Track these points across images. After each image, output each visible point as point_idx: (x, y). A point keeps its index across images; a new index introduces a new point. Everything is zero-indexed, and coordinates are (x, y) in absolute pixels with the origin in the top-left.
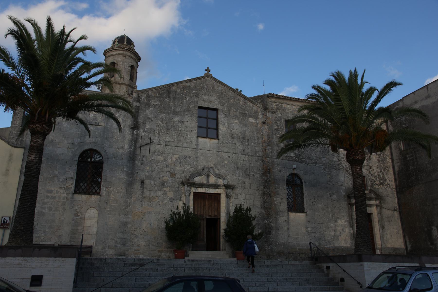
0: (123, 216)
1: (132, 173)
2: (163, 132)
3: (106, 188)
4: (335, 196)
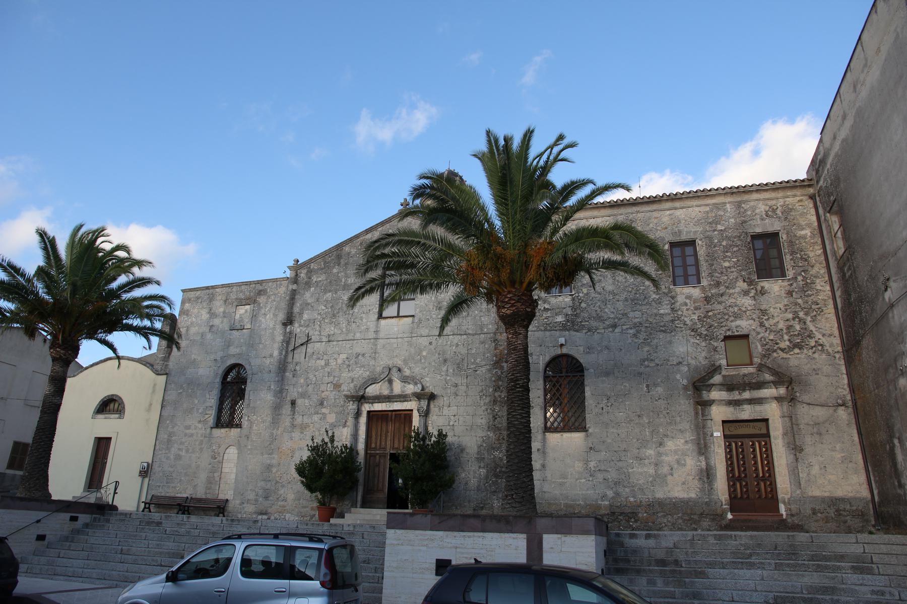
1: (281, 391)
4: (660, 390)
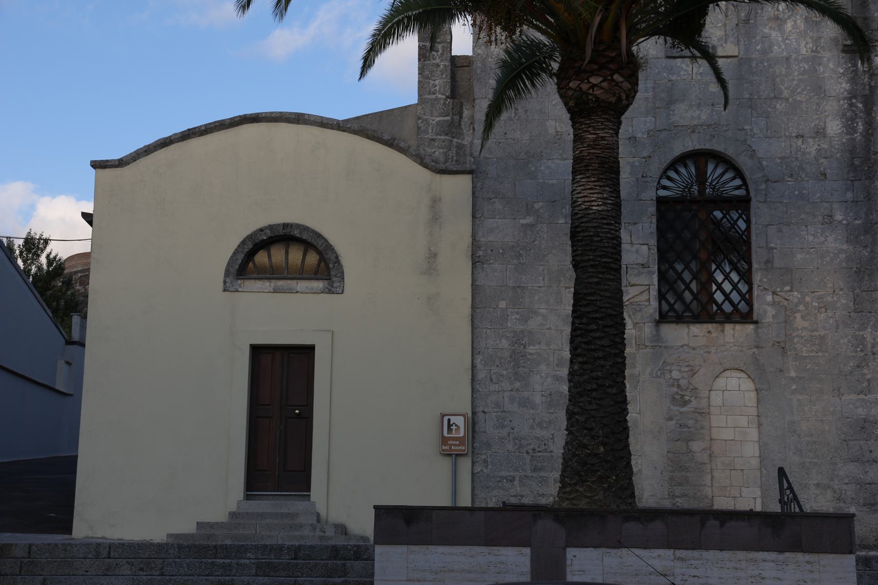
0: (853, 397)
3: (774, 293)
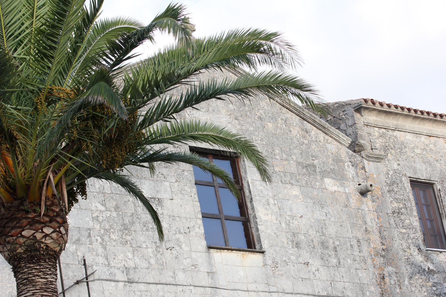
2: (113, 237)
